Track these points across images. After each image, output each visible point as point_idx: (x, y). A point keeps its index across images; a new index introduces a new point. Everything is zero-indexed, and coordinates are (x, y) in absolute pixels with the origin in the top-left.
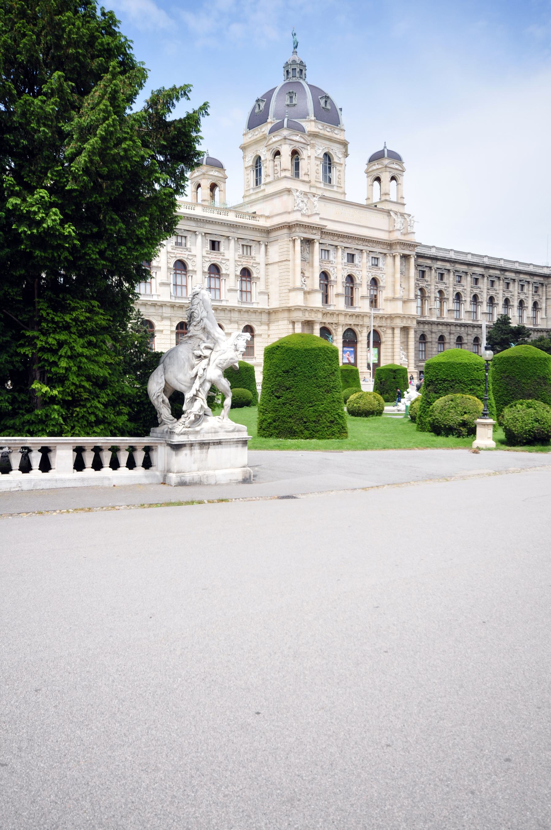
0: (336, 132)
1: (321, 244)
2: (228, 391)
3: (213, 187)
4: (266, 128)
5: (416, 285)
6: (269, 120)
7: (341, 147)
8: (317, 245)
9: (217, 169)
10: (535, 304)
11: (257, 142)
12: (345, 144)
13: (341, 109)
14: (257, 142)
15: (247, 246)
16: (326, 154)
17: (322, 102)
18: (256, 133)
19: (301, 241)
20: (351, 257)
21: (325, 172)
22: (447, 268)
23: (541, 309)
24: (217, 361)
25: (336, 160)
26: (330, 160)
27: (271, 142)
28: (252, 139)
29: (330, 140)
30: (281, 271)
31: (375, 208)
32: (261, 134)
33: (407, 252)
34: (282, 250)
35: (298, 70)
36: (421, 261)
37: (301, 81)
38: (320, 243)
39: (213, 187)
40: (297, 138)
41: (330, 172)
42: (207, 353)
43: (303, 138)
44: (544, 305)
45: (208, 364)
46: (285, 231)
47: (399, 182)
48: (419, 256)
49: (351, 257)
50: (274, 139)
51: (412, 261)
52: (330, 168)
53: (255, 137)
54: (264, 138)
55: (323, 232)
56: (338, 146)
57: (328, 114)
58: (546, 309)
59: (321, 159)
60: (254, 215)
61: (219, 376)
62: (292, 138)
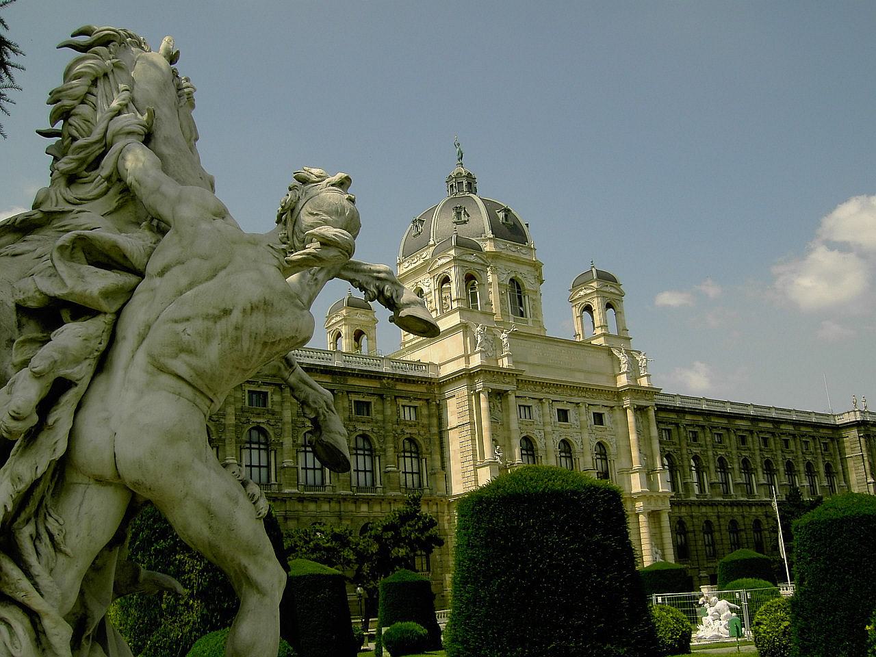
0: (524, 251)
1: (518, 397)
2: (253, 552)
3: (358, 335)
4: (427, 254)
5: (662, 451)
6: (432, 242)
7: (533, 269)
8: (512, 398)
9: (363, 311)
10: (828, 467)
11: (416, 272)
12: (537, 266)
13: (527, 225)
14: (416, 272)
15: (410, 407)
16: (512, 280)
17: (501, 215)
18: (415, 261)
19: (489, 393)
20: (563, 415)
21: (513, 302)
22: (700, 423)
23: (837, 473)
24: (160, 334)
25: (527, 286)
26: (519, 287)
27: (436, 266)
28: (410, 267)
29: (517, 261)
30: (462, 439)
31: (589, 345)
32: (422, 261)
33: (643, 403)
34: (461, 410)
35: (465, 183)
36: (662, 415)
37: (471, 195)
38: (516, 397)
39: (358, 335)
40: (472, 258)
41: (521, 305)
42: (94, 283)
43: (480, 258)
44: (840, 468)
45: (103, 363)
46: (465, 382)
47: (618, 309)
48: (661, 409)
49: (563, 415)
50: (440, 262)
51: (652, 413)
52: (520, 298)
53: (414, 266)
54: (426, 263)
55: (521, 382)
56: (529, 268)
57: (510, 230)
58: (844, 472)
59: (506, 285)
60: (418, 364)
61: (172, 438)
62: (464, 257)
